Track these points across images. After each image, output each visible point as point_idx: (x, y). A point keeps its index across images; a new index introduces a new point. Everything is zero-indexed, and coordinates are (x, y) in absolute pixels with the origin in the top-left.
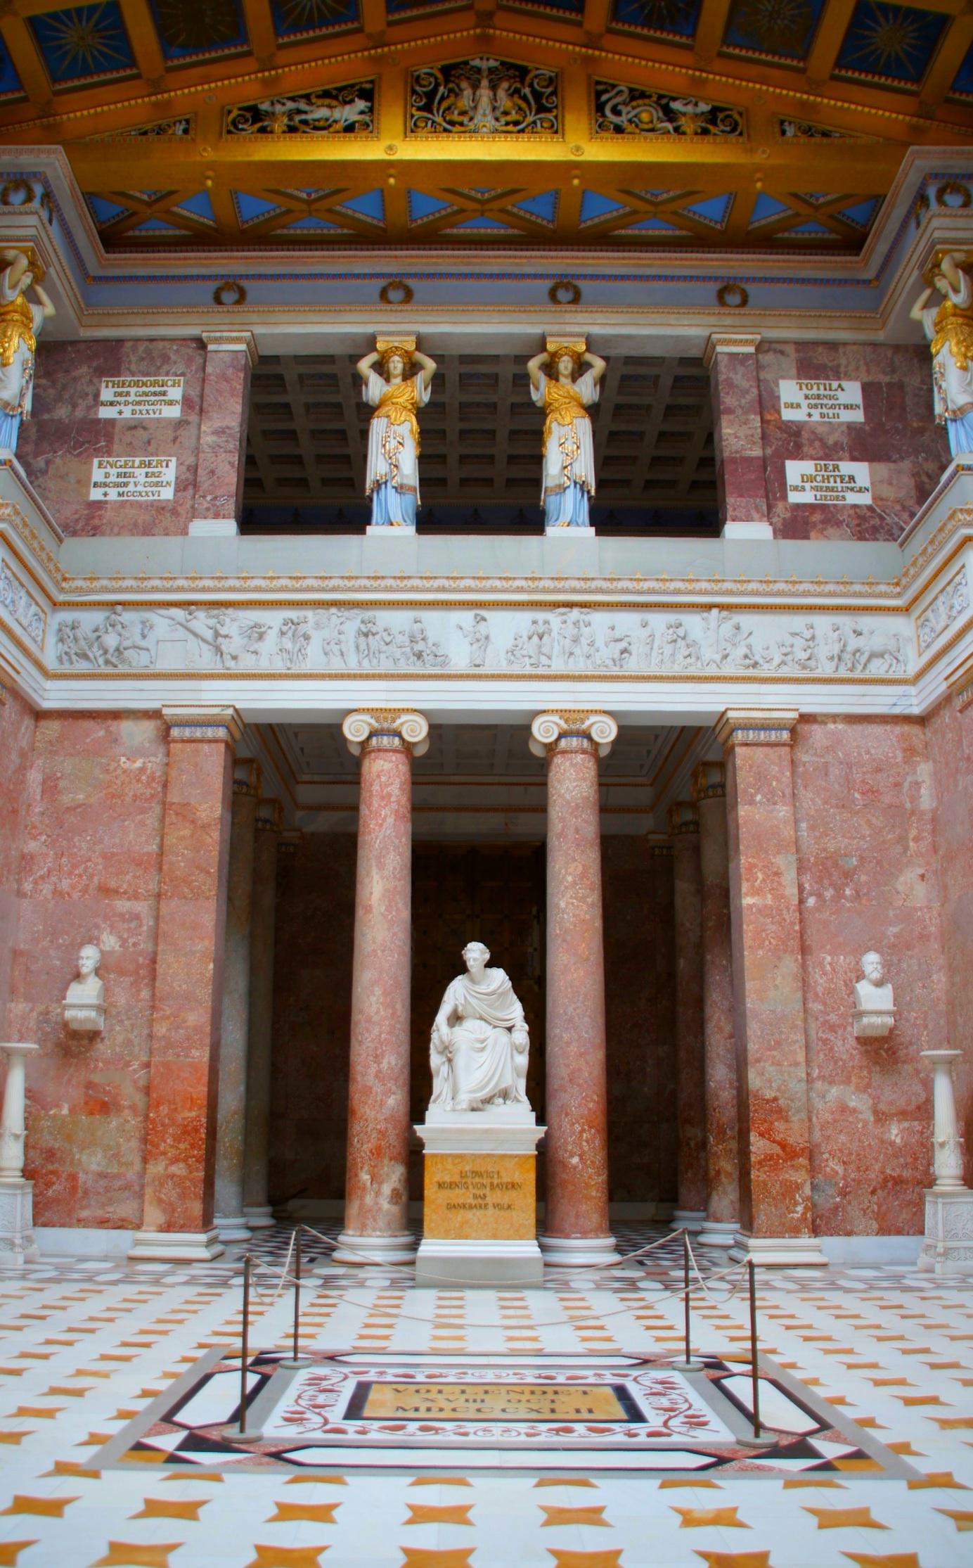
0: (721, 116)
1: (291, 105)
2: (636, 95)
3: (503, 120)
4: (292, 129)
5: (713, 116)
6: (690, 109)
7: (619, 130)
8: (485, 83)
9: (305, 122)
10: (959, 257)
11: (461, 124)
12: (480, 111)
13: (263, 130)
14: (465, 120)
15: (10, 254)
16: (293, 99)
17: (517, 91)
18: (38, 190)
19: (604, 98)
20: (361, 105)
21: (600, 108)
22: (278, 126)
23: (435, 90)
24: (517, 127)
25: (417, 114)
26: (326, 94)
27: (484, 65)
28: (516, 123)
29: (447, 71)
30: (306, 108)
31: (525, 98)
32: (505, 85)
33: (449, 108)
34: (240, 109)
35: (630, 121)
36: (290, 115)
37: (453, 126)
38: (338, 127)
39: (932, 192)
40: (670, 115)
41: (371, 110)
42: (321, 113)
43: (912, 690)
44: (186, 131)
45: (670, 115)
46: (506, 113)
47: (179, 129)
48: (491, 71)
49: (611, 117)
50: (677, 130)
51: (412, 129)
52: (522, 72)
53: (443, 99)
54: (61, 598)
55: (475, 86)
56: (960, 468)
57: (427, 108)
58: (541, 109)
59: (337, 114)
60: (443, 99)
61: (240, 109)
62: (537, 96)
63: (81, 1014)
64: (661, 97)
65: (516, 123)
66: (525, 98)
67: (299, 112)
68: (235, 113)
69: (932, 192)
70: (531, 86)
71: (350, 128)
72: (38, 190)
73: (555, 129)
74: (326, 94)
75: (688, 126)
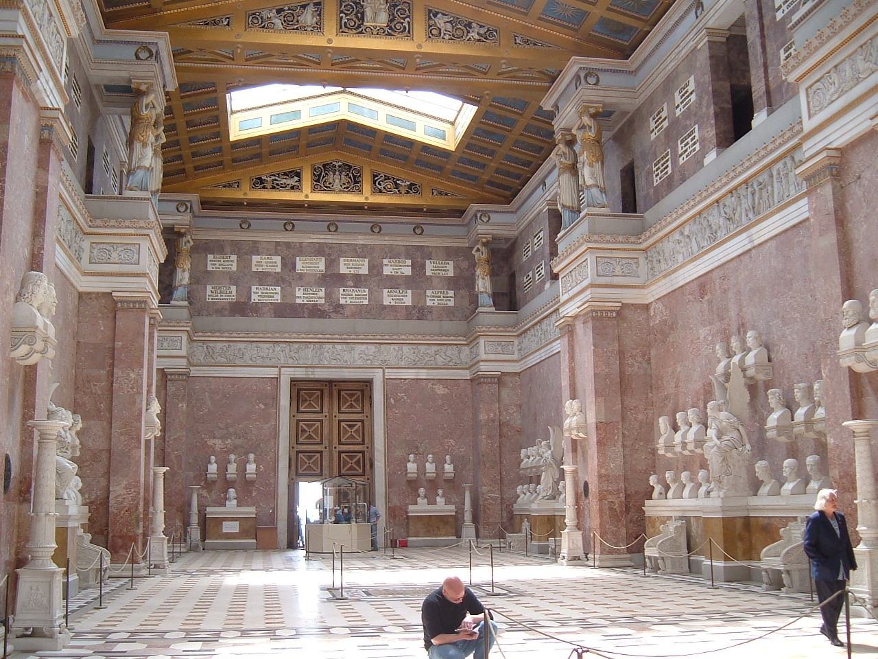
0: (413, 187)
1: (273, 178)
2: (387, 178)
3: (343, 186)
4: (274, 187)
5: (411, 186)
6: (403, 184)
7: (380, 191)
8: (337, 173)
9: (277, 185)
10: (484, 240)
11: (329, 187)
12: (335, 184)
13: (264, 187)
14: (331, 186)
15: (183, 231)
16: (274, 175)
17: (348, 175)
18: (189, 205)
19: (376, 178)
20: (296, 179)
21: (374, 182)
22: (269, 186)
23: (321, 174)
24: (347, 189)
25: (315, 183)
26: (285, 174)
27: (337, 164)
28: (348, 188)
29: (324, 166)
30: (277, 178)
31: (350, 178)
32: (344, 173)
33: (325, 181)
34: (256, 179)
35: (384, 188)
36: (273, 180)
37: (328, 188)
38: (288, 187)
39: (479, 216)
40: (397, 186)
41: (300, 180)
42: (284, 181)
43: (468, 371)
44: (238, 186)
45: (397, 186)
46: (344, 184)
47: (236, 185)
48: (340, 166)
49: (379, 187)
50: (399, 191)
51: (313, 190)
52: (350, 167)
53: (324, 177)
54: (195, 339)
55: (334, 174)
56: (479, 312)
57: (318, 181)
58: (356, 182)
59: (288, 182)
60: (324, 177)
61: (256, 179)
62: (354, 177)
63: (213, 476)
64: (394, 179)
65: (348, 188)
66: (350, 178)
67: (276, 180)
68: (255, 180)
69: (479, 216)
70: (352, 173)
71: (293, 188)
72: (189, 205)
73: (360, 191)
74: (285, 174)
75: (403, 190)
